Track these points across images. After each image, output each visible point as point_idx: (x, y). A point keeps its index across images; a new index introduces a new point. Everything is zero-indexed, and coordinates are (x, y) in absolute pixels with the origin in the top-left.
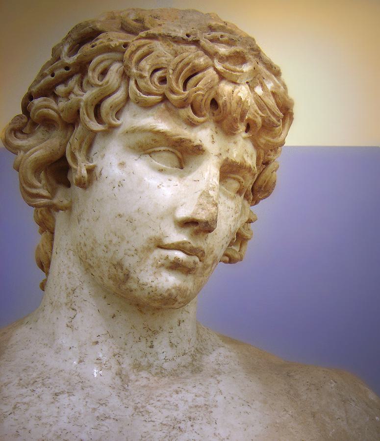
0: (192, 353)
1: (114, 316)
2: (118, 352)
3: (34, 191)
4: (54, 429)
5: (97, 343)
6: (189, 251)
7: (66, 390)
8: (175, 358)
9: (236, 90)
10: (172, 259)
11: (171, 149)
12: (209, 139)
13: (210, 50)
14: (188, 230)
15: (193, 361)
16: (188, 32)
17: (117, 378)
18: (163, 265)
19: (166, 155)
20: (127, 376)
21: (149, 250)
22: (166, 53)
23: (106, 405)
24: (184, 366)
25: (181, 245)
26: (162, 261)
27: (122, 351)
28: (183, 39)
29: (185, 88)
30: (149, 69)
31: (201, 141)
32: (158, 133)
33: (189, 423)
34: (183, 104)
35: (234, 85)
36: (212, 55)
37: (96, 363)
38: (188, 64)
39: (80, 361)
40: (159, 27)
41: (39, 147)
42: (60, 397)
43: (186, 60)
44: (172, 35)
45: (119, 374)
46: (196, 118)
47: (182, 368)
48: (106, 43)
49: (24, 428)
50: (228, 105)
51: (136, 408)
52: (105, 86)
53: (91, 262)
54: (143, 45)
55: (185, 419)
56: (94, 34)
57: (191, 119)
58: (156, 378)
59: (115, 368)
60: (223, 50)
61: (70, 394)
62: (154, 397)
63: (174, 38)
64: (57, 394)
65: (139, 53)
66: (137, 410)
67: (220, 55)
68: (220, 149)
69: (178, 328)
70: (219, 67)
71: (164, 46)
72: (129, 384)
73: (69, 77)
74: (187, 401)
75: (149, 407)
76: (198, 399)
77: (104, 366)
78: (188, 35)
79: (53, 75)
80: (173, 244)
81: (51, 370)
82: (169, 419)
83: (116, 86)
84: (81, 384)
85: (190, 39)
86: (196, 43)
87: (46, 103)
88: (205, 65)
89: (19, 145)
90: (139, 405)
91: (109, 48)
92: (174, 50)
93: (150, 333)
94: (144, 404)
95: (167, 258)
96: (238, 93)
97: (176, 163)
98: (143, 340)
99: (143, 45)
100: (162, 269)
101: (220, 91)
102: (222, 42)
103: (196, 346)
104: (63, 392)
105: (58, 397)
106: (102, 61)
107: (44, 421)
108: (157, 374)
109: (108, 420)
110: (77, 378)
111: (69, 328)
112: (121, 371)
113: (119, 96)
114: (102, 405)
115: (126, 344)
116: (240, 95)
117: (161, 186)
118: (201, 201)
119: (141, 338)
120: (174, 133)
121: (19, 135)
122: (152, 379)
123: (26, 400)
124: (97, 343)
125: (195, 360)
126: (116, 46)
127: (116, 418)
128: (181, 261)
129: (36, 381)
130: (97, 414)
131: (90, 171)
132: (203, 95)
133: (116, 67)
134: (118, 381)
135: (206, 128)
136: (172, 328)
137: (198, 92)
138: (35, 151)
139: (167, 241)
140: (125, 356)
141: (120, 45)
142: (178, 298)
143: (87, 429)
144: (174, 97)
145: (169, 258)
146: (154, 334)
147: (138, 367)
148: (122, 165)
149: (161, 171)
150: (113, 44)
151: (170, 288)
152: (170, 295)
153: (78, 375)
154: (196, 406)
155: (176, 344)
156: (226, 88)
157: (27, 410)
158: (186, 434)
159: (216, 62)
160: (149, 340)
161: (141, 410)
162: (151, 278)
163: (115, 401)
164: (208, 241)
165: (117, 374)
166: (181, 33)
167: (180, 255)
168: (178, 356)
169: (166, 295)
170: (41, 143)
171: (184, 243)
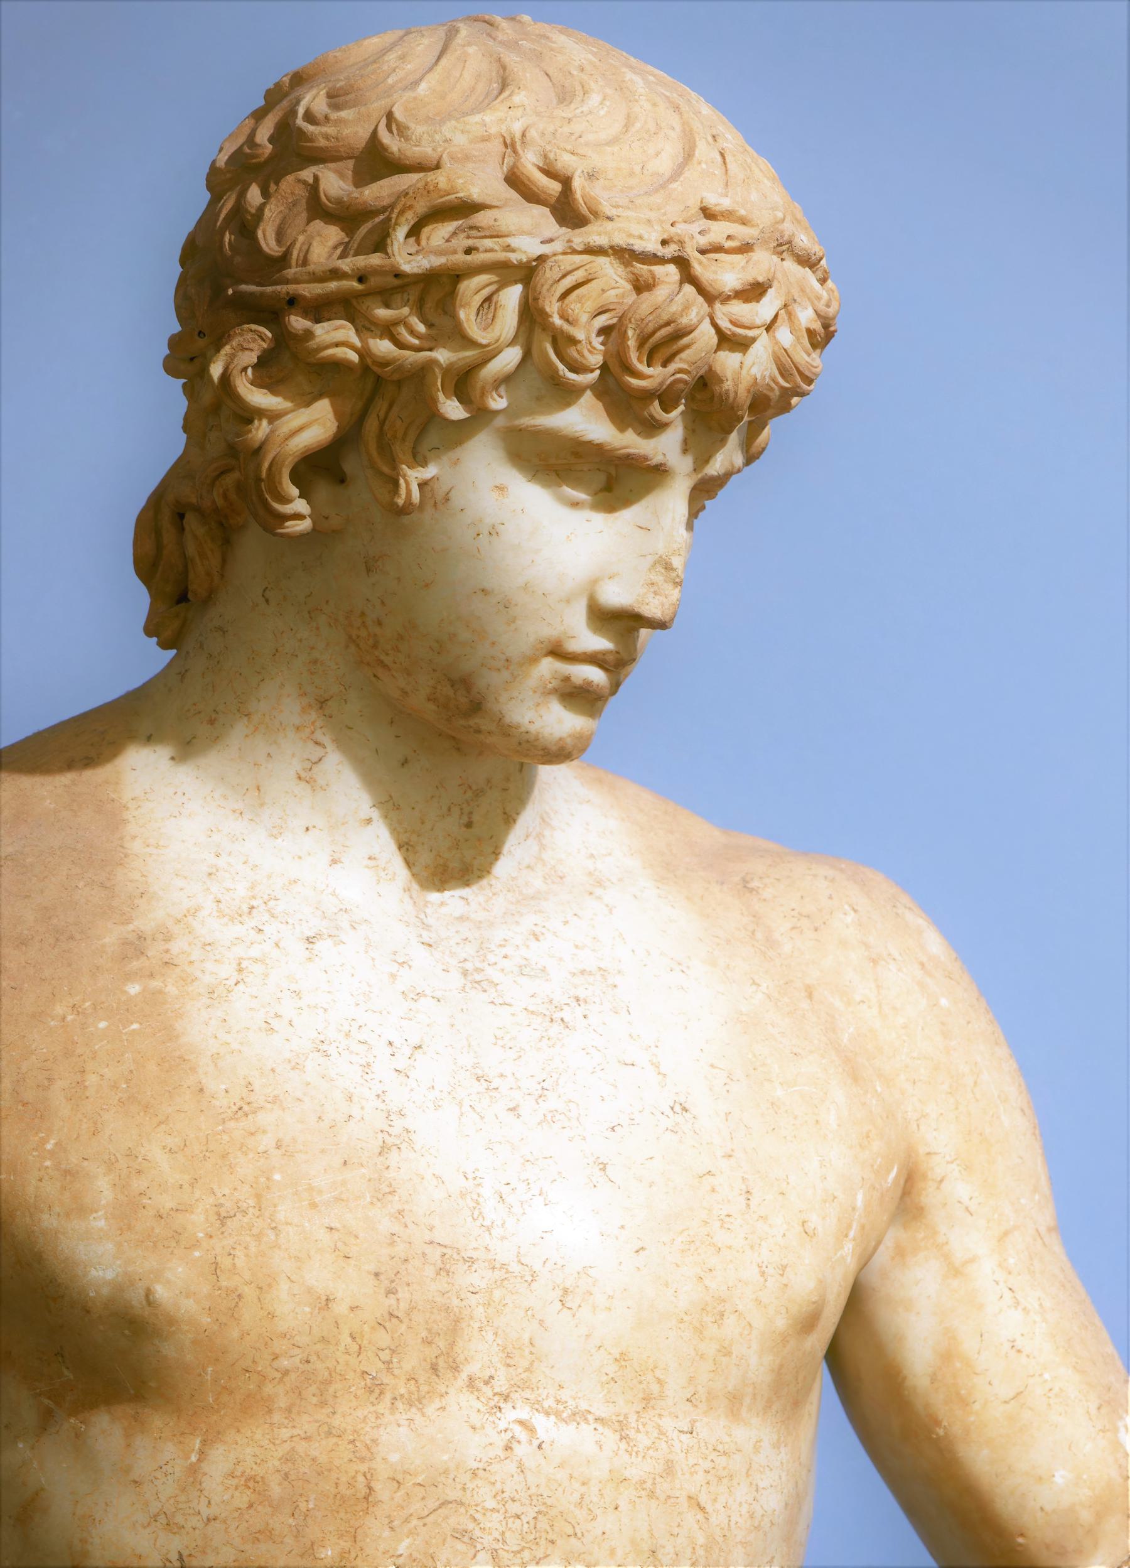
1: (405, 762)
3: (287, 509)
7: (325, 931)
13: (709, 289)
16: (665, 236)
18: (555, 691)
25: (600, 656)
26: (555, 683)
27: (414, 838)
33: (579, 1011)
34: (647, 396)
36: (709, 296)
37: (367, 867)
38: (668, 324)
39: (334, 862)
40: (609, 225)
42: (319, 946)
43: (665, 317)
44: (636, 248)
48: (502, 256)
49: (277, 1016)
50: (732, 396)
51: (465, 973)
53: (388, 660)
55: (568, 1001)
56: (465, 209)
60: (728, 275)
62: (493, 947)
64: (309, 940)
65: (568, 282)
66: (469, 978)
70: (724, 324)
72: (429, 911)
73: (401, 289)
74: (561, 959)
75: (490, 972)
77: (382, 874)
78: (664, 243)
79: (361, 280)
81: (269, 877)
85: (670, 251)
86: (681, 262)
87: (339, 335)
89: (263, 406)
90: (469, 966)
93: (469, 794)
94: (479, 965)
95: (567, 679)
98: (456, 811)
101: (718, 368)
105: (316, 947)
106: (488, 285)
109: (422, 1000)
111: (303, 784)
113: (511, 357)
118: (654, 577)
123: (255, 952)
126: (520, 262)
127: (438, 994)
129: (253, 907)
131: (422, 485)
133: (512, 295)
136: (508, 780)
138: (301, 429)
139: (574, 646)
144: (635, 382)
145: (573, 679)
148: (501, 489)
149: (575, 504)
150: (514, 258)
151: (565, 735)
154: (583, 972)
156: (728, 362)
161: (478, 977)
166: (650, 244)
167: (595, 675)
169: (554, 748)
171: (604, 653)
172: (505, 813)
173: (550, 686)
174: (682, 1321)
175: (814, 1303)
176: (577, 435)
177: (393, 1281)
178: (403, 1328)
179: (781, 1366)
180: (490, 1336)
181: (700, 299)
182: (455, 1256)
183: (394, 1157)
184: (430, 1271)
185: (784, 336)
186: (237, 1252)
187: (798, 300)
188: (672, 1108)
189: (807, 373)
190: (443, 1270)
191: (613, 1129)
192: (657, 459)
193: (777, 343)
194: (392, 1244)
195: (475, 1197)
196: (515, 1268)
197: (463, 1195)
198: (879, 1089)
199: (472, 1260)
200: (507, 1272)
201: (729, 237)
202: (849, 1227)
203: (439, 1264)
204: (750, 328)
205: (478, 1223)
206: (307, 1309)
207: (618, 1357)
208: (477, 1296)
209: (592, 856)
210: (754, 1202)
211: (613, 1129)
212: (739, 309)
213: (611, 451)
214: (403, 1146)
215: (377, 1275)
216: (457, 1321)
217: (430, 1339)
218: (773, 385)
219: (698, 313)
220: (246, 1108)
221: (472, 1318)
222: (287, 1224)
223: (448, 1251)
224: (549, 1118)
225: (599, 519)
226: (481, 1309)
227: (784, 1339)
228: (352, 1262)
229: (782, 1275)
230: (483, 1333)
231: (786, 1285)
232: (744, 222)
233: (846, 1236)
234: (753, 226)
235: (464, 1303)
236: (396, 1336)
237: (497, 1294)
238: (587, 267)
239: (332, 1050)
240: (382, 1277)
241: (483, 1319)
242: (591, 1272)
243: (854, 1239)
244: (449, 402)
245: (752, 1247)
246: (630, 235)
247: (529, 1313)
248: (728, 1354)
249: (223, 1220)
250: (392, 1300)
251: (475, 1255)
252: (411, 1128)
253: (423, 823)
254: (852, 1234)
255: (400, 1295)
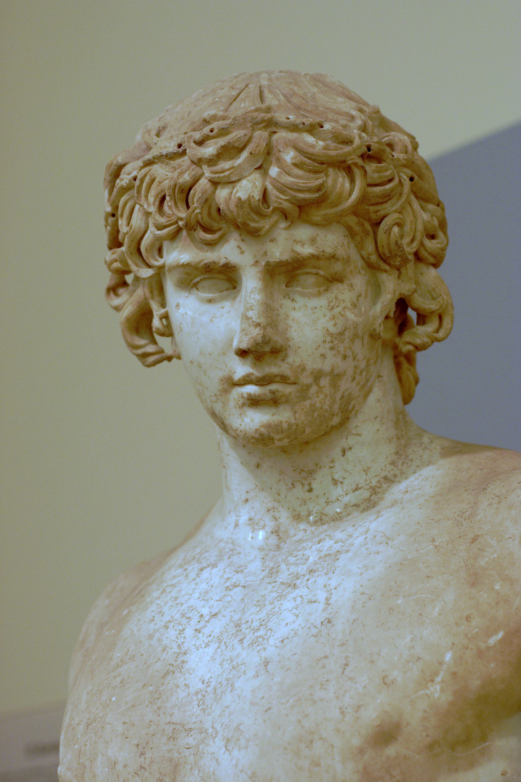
0: (374, 483)
1: (258, 466)
2: (272, 506)
3: (140, 351)
4: (184, 607)
5: (247, 500)
6: (261, 382)
8: (339, 498)
9: (234, 191)
10: (245, 396)
11: (206, 276)
12: (237, 251)
14: (250, 358)
15: (371, 495)
16: (179, 142)
17: (274, 536)
18: (244, 404)
19: (205, 283)
20: (286, 532)
21: (225, 391)
22: (167, 173)
23: (242, 572)
24: (355, 505)
25: (248, 379)
27: (276, 504)
28: (175, 153)
29: (188, 207)
30: (155, 201)
31: (226, 258)
32: (183, 265)
35: (231, 186)
37: (248, 525)
41: (128, 302)
42: (204, 571)
45: (276, 532)
46: (208, 237)
47: (351, 508)
52: (131, 232)
54: (145, 176)
57: (204, 240)
58: (313, 528)
59: (271, 525)
61: (214, 566)
63: (166, 156)
67: (206, 159)
68: (255, 256)
69: (342, 459)
71: (164, 167)
72: (288, 541)
76: (335, 545)
80: (239, 379)
82: (291, 576)
83: (143, 226)
84: (230, 552)
85: (181, 150)
88: (191, 180)
91: (124, 189)
92: (173, 167)
93: (304, 474)
96: (236, 193)
97: (226, 285)
98: (299, 486)
99: (145, 176)
100: (246, 408)
102: (214, 137)
103: (384, 474)
104: (209, 566)
107: (178, 601)
108: (316, 522)
109: (236, 589)
110: (231, 546)
112: (279, 527)
114: (237, 572)
115: (279, 495)
116: (239, 194)
117: (214, 319)
119: (294, 483)
120: (197, 260)
121: (121, 291)
122: (310, 529)
123: (174, 582)
124: (247, 500)
125: (376, 493)
128: (254, 396)
130: (228, 584)
132: (201, 213)
134: (273, 540)
135: (227, 241)
136: (333, 461)
137: (196, 211)
140: (281, 509)
141: (130, 181)
142: (272, 435)
143: (212, 602)
146: (311, 474)
147: (297, 518)
149: (210, 301)
151: (257, 427)
152: (261, 435)
153: (233, 543)
155: (341, 480)
157: (170, 592)
158: (297, 591)
159: (205, 167)
160: (306, 483)
162: (239, 421)
163: (255, 566)
164: (290, 360)
165: (272, 533)
167: (251, 389)
168: (344, 494)
169: (257, 436)
170: (131, 296)
171: (248, 375)
172: (333, 480)
173: (240, 402)
174: (286, 749)
175: (377, 726)
176: (177, 262)
177: (144, 748)
178: (147, 774)
179: (365, 768)
180: (196, 772)
181: (194, 166)
182: (181, 729)
183: (169, 677)
184: (164, 739)
185: (274, 171)
186: (88, 743)
187: (282, 150)
188: (322, 623)
189: (295, 187)
190: (173, 738)
191: (282, 641)
192: (223, 261)
193: (271, 177)
194: (149, 726)
195: (204, 693)
196: (210, 730)
197: (197, 693)
198: (497, 587)
199: (191, 730)
200: (207, 733)
201: (212, 131)
202: (436, 674)
203: (171, 735)
204: (223, 172)
205: (200, 708)
206: (107, 770)
207: (251, 775)
208: (190, 750)
209: (407, 491)
210: (348, 669)
211: (282, 641)
212: (225, 165)
213: (197, 264)
214: (176, 672)
215: (138, 745)
216: (176, 766)
217: (161, 778)
218: (279, 200)
219: (189, 175)
220: (120, 664)
221: (185, 763)
222: (109, 724)
223: (177, 727)
224: (254, 642)
225: (227, 304)
226: (192, 757)
227: (361, 751)
228: (128, 740)
229: (357, 712)
230: (193, 771)
231: (358, 718)
232: (224, 118)
233: (432, 681)
234: (230, 118)
235: (182, 755)
236: (143, 779)
237: (201, 747)
238: (149, 173)
239: (171, 625)
240: (140, 746)
241: (193, 763)
242: (242, 727)
243: (442, 681)
244: (141, 270)
245: (337, 698)
246: (161, 148)
247: (213, 756)
248: (318, 765)
249: (88, 725)
250: (142, 759)
251: (192, 726)
252: (186, 660)
253: (279, 495)
254: (439, 679)
255: (146, 755)
